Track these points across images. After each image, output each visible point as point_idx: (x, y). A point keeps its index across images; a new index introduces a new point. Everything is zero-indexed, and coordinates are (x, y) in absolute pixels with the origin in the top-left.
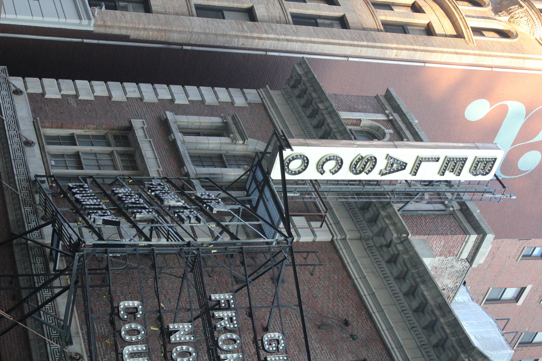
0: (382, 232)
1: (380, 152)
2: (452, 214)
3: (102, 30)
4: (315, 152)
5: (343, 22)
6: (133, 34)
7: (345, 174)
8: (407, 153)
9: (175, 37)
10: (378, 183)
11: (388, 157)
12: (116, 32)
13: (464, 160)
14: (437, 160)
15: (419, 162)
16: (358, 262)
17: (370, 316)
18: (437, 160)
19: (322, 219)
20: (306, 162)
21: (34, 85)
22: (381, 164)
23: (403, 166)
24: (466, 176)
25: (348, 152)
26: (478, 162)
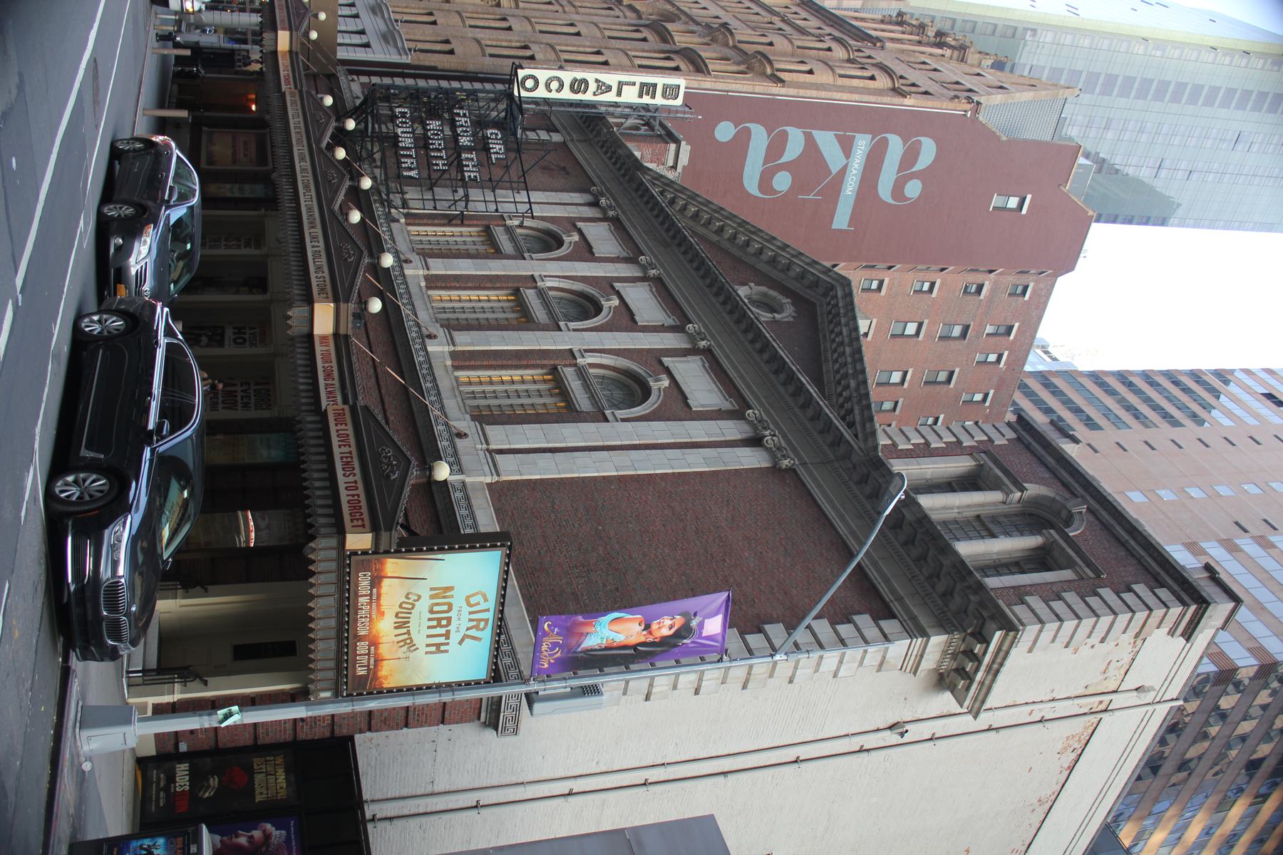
0: (599, 134)
1: (591, 76)
2: (660, 136)
3: (416, 63)
4: (543, 75)
5: (606, 63)
6: (440, 67)
7: (566, 94)
8: (611, 78)
9: (471, 67)
10: (593, 105)
11: (597, 81)
12: (427, 64)
13: (655, 86)
14: (634, 84)
15: (621, 84)
16: (580, 152)
17: (582, 167)
18: (634, 84)
19: (557, 131)
20: (537, 82)
21: (364, 79)
22: (593, 86)
23: (609, 88)
24: (659, 100)
25: (567, 76)
26: (665, 87)
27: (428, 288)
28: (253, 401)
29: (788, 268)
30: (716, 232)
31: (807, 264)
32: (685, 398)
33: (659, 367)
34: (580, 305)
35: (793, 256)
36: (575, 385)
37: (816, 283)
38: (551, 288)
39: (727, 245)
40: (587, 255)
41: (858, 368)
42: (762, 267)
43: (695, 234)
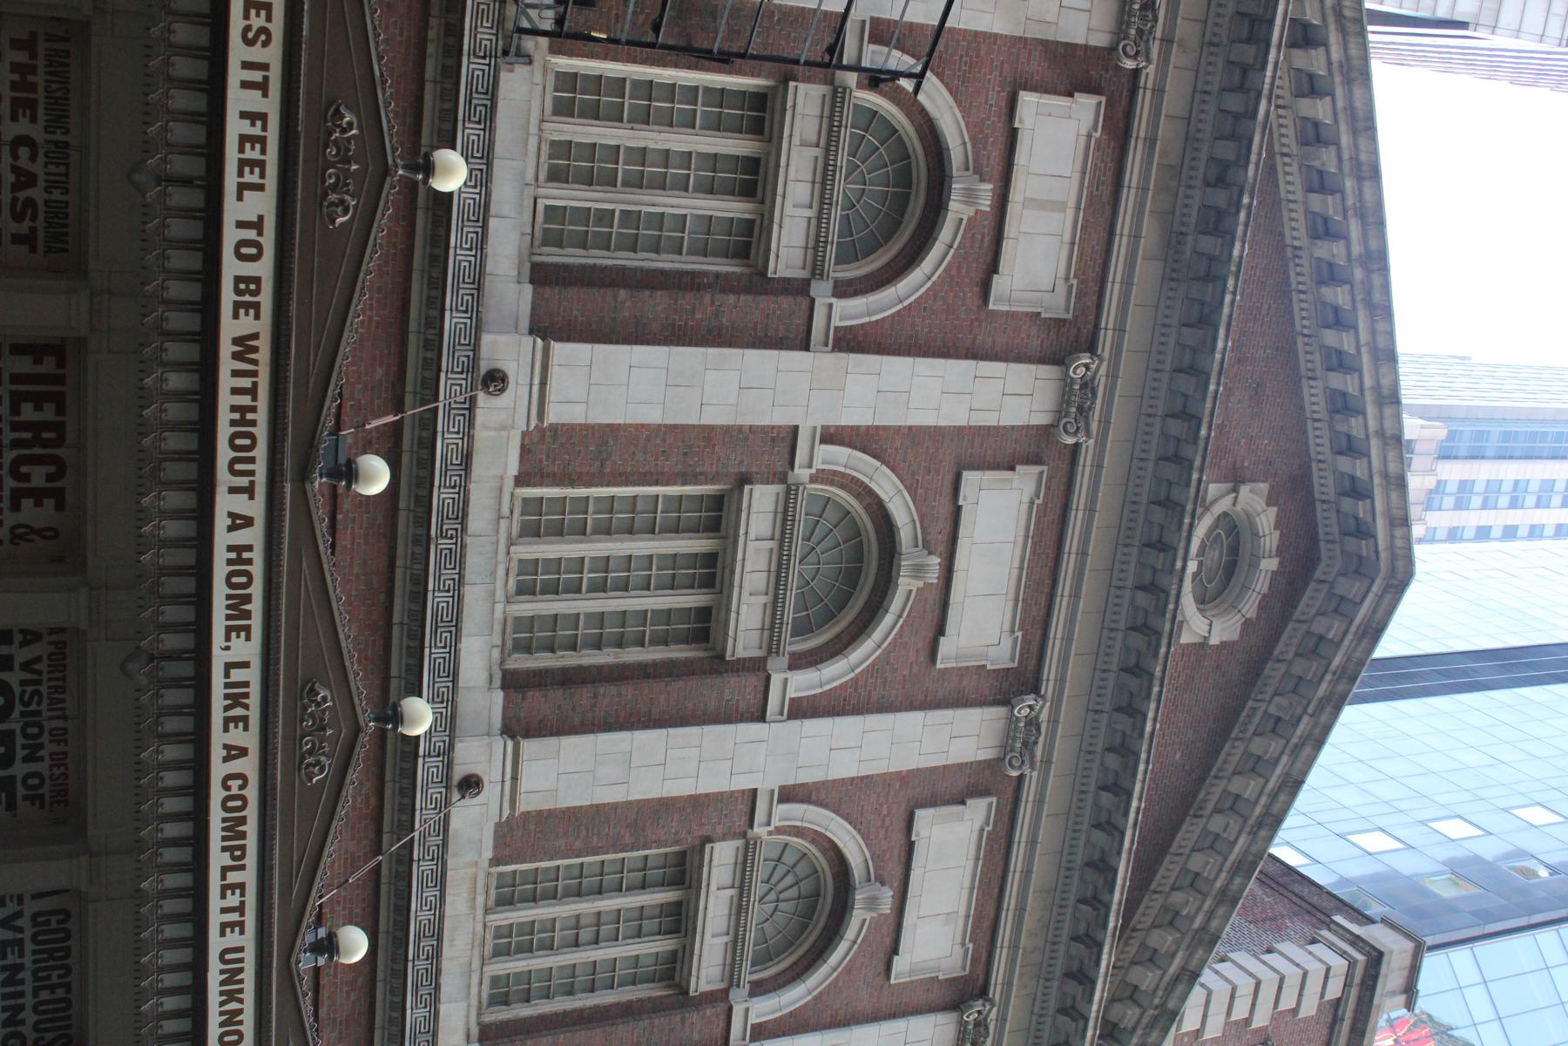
27: (520, 481)
28: (28, 960)
29: (1350, 447)
30: (1311, 215)
31: (1385, 475)
32: (895, 950)
33: (899, 823)
34: (858, 555)
35: (1381, 433)
36: (715, 908)
37: (1363, 531)
38: (821, 477)
39: (1301, 275)
40: (971, 296)
41: (1214, 924)
42: (1314, 398)
43: (1271, 170)
